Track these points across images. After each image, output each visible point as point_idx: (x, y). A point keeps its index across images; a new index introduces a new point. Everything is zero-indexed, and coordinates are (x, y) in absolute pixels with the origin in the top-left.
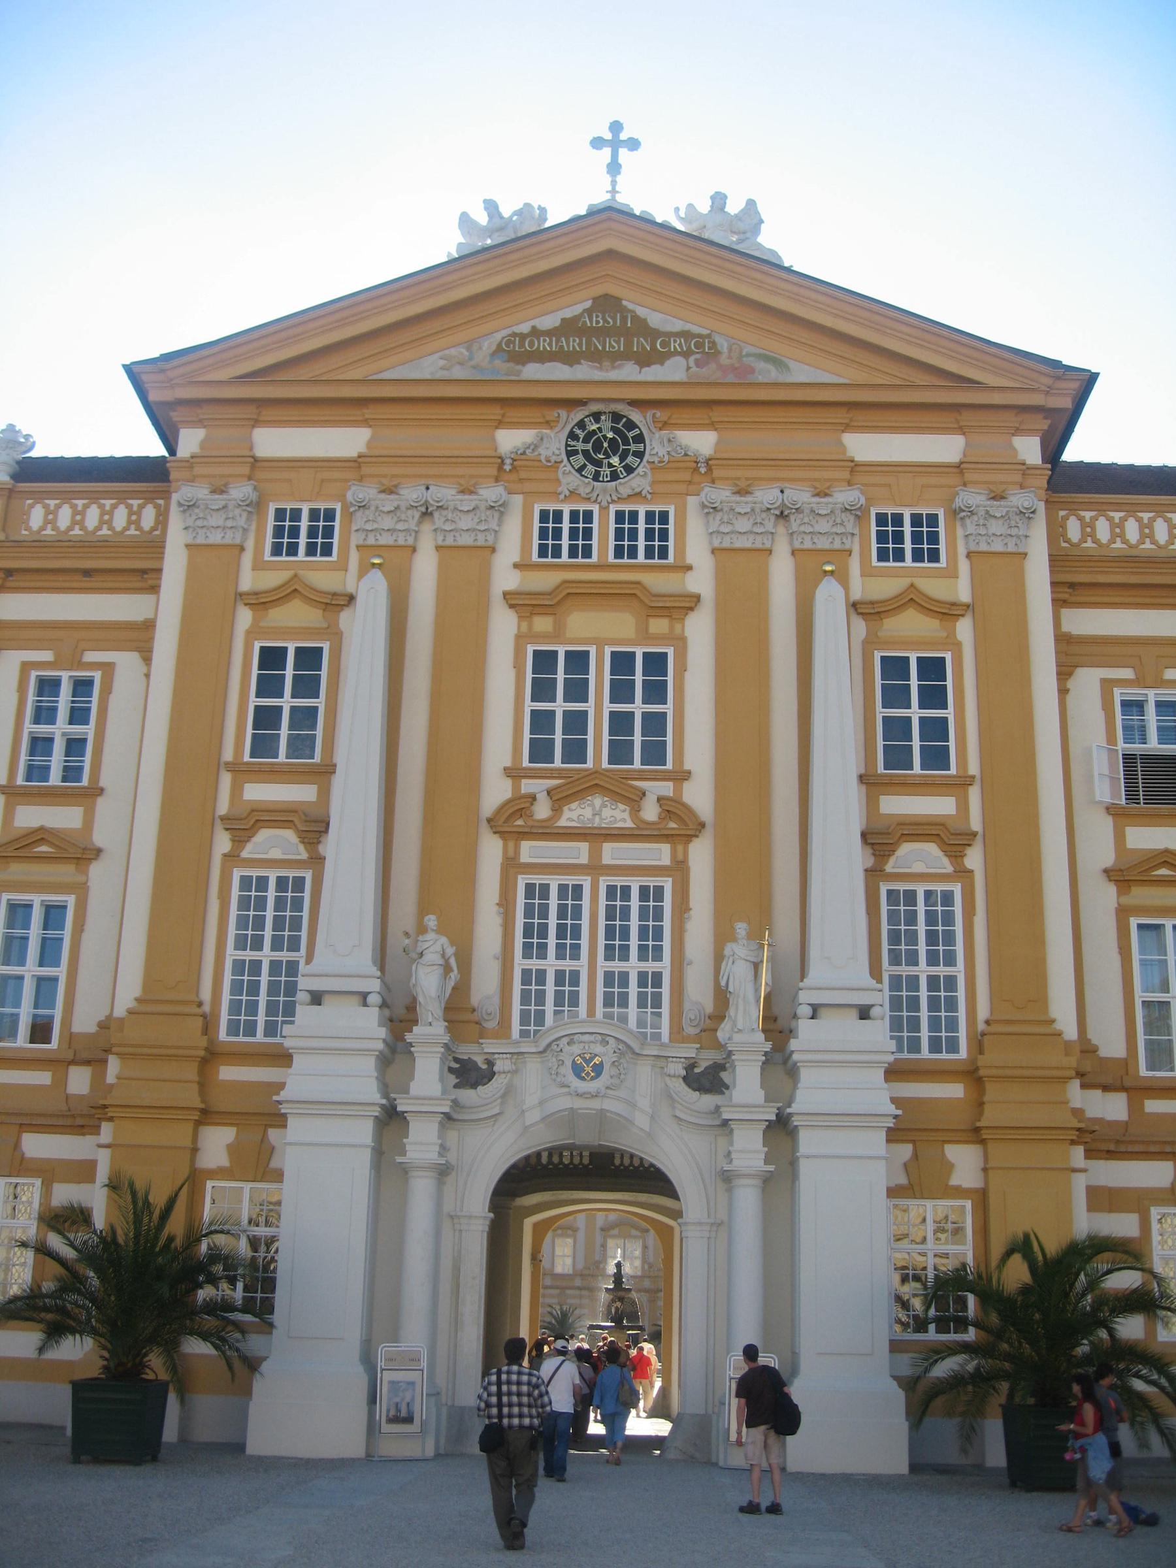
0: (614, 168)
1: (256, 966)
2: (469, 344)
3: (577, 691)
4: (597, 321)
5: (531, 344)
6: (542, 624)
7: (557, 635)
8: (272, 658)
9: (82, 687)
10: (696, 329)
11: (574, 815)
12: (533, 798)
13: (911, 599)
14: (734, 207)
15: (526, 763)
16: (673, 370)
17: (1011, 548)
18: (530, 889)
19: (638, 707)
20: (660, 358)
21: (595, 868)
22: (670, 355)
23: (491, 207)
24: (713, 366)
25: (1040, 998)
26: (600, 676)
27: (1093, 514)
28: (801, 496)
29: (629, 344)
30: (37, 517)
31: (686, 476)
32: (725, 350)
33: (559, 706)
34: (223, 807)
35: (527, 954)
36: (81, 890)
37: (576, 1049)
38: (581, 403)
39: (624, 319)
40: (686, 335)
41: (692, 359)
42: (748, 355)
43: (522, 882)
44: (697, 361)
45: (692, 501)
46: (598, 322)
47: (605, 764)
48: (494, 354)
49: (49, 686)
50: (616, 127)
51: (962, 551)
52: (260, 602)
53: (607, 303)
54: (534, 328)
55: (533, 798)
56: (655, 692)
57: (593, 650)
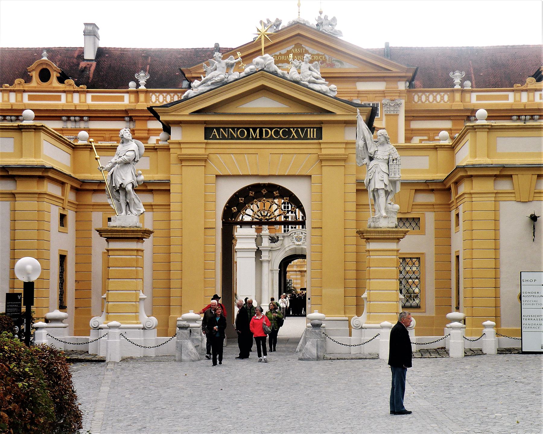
0: (299, 6)
5: (280, 57)
10: (321, 53)
14: (330, 18)
17: (395, 113)
24: (325, 64)
27: (421, 94)
30: (154, 98)
37: (296, 235)
40: (318, 55)
41: (319, 62)
42: (334, 60)
44: (321, 62)
46: (296, 51)
51: (384, 114)
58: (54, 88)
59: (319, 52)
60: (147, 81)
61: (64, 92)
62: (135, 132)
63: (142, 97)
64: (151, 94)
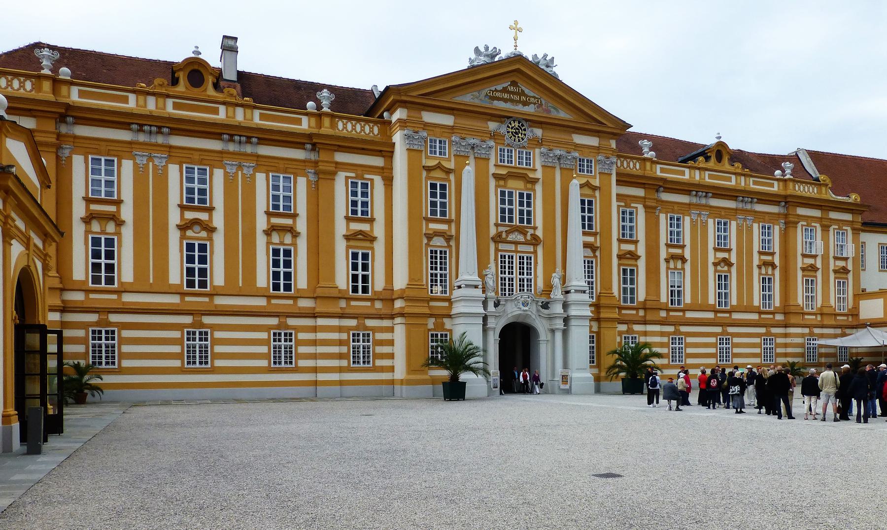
1: (436, 275)
2: (479, 91)
3: (511, 203)
4: (511, 89)
6: (502, 183)
8: (433, 186)
9: (365, 186)
10: (537, 96)
11: (511, 237)
12: (502, 232)
15: (499, 222)
18: (501, 256)
19: (525, 208)
21: (516, 251)
23: (487, 48)
24: (541, 108)
25: (610, 288)
26: (516, 199)
29: (520, 98)
31: (536, 143)
32: (544, 104)
33: (507, 206)
34: (424, 231)
35: (501, 273)
36: (372, 249)
38: (511, 117)
39: (519, 90)
40: (534, 97)
43: (500, 254)
45: (537, 151)
47: (518, 224)
48: (485, 96)
49: (354, 185)
51: (598, 172)
52: (429, 169)
54: (495, 89)
55: (502, 232)
56: (529, 205)
58: (209, 96)
59: (535, 95)
60: (332, 103)
61: (224, 103)
62: (320, 164)
63: (326, 121)
64: (337, 119)
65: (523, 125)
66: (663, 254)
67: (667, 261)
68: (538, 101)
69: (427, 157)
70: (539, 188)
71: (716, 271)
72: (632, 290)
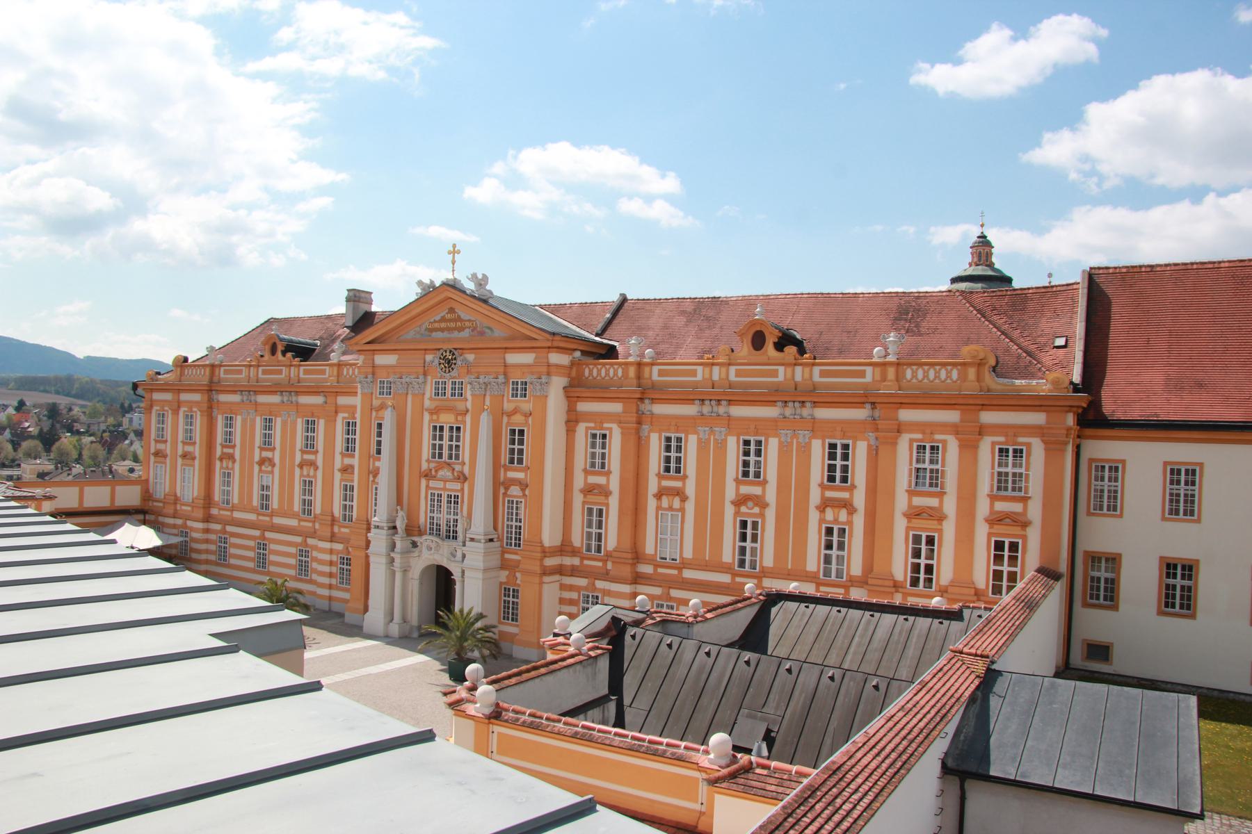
4: (449, 316)
6: (435, 417)
7: (437, 421)
10: (473, 319)
13: (515, 411)
14: (480, 276)
16: (466, 333)
20: (461, 329)
21: (445, 489)
22: (466, 328)
24: (476, 332)
26: (446, 434)
28: (490, 379)
29: (456, 325)
40: (469, 321)
48: (426, 330)
50: (454, 246)
53: (452, 310)
57: (445, 425)
65: (453, 354)
66: (653, 485)
67: (659, 496)
68: (472, 324)
69: (377, 398)
70: (468, 418)
71: (737, 513)
72: (599, 536)
